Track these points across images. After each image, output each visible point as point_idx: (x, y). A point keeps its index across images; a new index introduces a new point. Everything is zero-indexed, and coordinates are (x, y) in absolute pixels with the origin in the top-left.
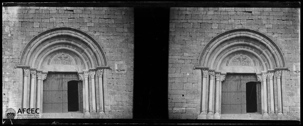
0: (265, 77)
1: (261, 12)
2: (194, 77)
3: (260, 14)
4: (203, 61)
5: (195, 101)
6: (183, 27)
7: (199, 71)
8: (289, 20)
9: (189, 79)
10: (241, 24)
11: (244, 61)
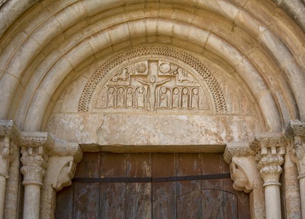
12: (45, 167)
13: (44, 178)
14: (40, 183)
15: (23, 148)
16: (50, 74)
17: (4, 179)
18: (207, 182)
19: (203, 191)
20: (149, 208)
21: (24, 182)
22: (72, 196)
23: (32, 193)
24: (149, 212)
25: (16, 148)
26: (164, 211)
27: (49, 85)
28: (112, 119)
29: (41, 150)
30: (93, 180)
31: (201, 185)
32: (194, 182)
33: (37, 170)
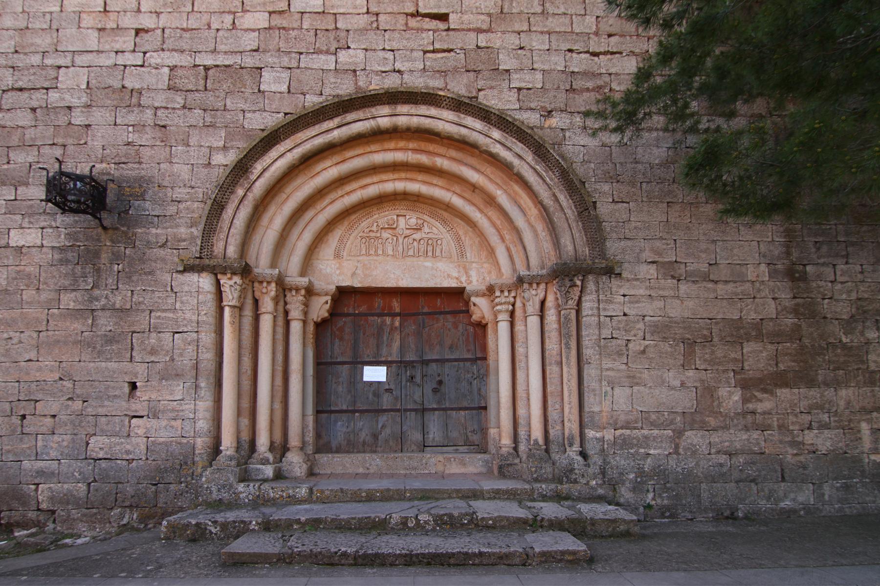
0: (505, 303)
1: (490, 15)
2: (178, 305)
3: (485, 27)
4: (223, 236)
5: (187, 406)
6: (123, 87)
7: (205, 282)
8: (620, 53)
9: (159, 314)
10: (399, 71)
11: (415, 236)
12: (306, 305)
13: (306, 313)
14: (304, 318)
15: (287, 290)
16: (308, 228)
17: (272, 316)
18: (449, 316)
19: (446, 324)
20: (399, 337)
21: (289, 318)
22: (330, 330)
23: (296, 327)
24: (398, 340)
25: (281, 290)
26: (411, 339)
27: (307, 237)
28: (364, 265)
29: (303, 292)
30: (348, 315)
31: (444, 319)
32: (436, 316)
33: (301, 309)
